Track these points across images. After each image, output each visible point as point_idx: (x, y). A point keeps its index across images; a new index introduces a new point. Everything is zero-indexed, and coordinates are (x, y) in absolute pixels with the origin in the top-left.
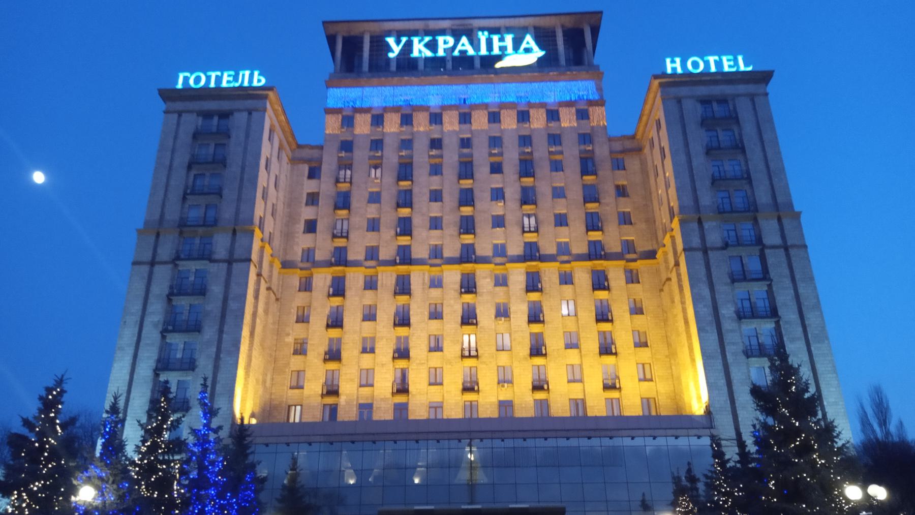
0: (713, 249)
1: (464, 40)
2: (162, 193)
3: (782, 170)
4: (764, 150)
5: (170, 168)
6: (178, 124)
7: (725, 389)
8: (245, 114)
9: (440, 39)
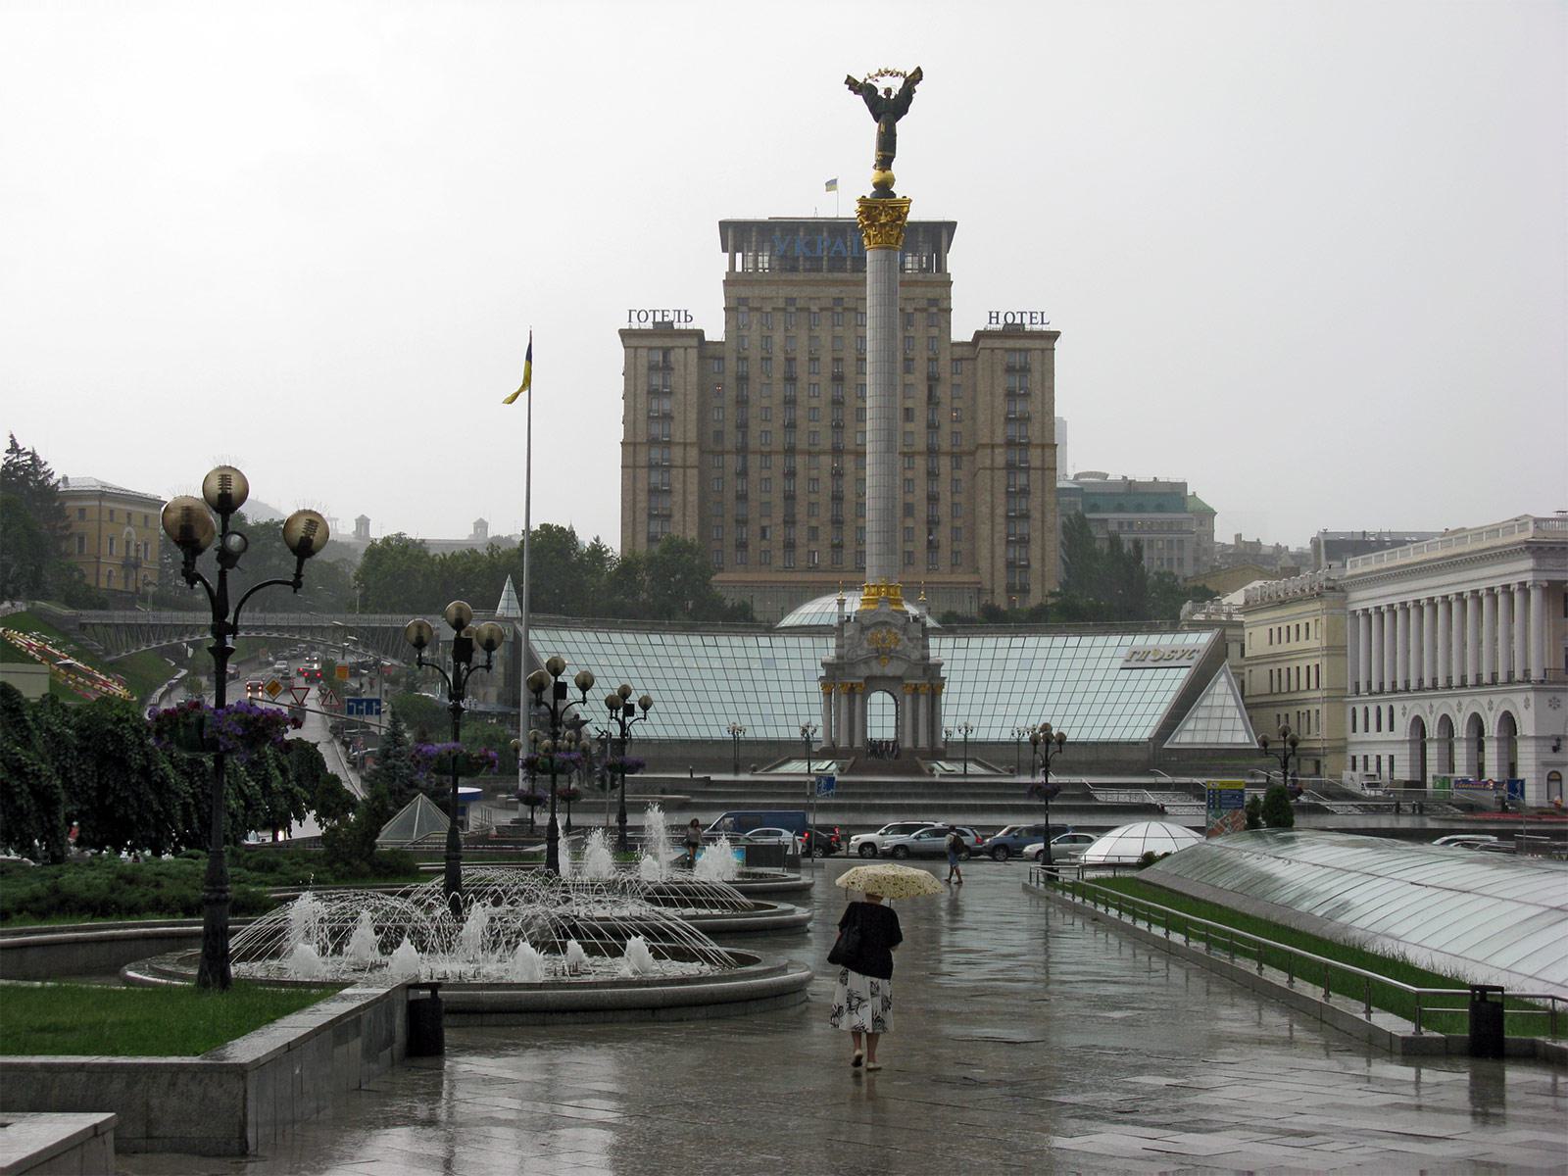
1: (839, 240)
4: (1043, 395)
5: (635, 395)
7: (989, 561)
8: (682, 350)
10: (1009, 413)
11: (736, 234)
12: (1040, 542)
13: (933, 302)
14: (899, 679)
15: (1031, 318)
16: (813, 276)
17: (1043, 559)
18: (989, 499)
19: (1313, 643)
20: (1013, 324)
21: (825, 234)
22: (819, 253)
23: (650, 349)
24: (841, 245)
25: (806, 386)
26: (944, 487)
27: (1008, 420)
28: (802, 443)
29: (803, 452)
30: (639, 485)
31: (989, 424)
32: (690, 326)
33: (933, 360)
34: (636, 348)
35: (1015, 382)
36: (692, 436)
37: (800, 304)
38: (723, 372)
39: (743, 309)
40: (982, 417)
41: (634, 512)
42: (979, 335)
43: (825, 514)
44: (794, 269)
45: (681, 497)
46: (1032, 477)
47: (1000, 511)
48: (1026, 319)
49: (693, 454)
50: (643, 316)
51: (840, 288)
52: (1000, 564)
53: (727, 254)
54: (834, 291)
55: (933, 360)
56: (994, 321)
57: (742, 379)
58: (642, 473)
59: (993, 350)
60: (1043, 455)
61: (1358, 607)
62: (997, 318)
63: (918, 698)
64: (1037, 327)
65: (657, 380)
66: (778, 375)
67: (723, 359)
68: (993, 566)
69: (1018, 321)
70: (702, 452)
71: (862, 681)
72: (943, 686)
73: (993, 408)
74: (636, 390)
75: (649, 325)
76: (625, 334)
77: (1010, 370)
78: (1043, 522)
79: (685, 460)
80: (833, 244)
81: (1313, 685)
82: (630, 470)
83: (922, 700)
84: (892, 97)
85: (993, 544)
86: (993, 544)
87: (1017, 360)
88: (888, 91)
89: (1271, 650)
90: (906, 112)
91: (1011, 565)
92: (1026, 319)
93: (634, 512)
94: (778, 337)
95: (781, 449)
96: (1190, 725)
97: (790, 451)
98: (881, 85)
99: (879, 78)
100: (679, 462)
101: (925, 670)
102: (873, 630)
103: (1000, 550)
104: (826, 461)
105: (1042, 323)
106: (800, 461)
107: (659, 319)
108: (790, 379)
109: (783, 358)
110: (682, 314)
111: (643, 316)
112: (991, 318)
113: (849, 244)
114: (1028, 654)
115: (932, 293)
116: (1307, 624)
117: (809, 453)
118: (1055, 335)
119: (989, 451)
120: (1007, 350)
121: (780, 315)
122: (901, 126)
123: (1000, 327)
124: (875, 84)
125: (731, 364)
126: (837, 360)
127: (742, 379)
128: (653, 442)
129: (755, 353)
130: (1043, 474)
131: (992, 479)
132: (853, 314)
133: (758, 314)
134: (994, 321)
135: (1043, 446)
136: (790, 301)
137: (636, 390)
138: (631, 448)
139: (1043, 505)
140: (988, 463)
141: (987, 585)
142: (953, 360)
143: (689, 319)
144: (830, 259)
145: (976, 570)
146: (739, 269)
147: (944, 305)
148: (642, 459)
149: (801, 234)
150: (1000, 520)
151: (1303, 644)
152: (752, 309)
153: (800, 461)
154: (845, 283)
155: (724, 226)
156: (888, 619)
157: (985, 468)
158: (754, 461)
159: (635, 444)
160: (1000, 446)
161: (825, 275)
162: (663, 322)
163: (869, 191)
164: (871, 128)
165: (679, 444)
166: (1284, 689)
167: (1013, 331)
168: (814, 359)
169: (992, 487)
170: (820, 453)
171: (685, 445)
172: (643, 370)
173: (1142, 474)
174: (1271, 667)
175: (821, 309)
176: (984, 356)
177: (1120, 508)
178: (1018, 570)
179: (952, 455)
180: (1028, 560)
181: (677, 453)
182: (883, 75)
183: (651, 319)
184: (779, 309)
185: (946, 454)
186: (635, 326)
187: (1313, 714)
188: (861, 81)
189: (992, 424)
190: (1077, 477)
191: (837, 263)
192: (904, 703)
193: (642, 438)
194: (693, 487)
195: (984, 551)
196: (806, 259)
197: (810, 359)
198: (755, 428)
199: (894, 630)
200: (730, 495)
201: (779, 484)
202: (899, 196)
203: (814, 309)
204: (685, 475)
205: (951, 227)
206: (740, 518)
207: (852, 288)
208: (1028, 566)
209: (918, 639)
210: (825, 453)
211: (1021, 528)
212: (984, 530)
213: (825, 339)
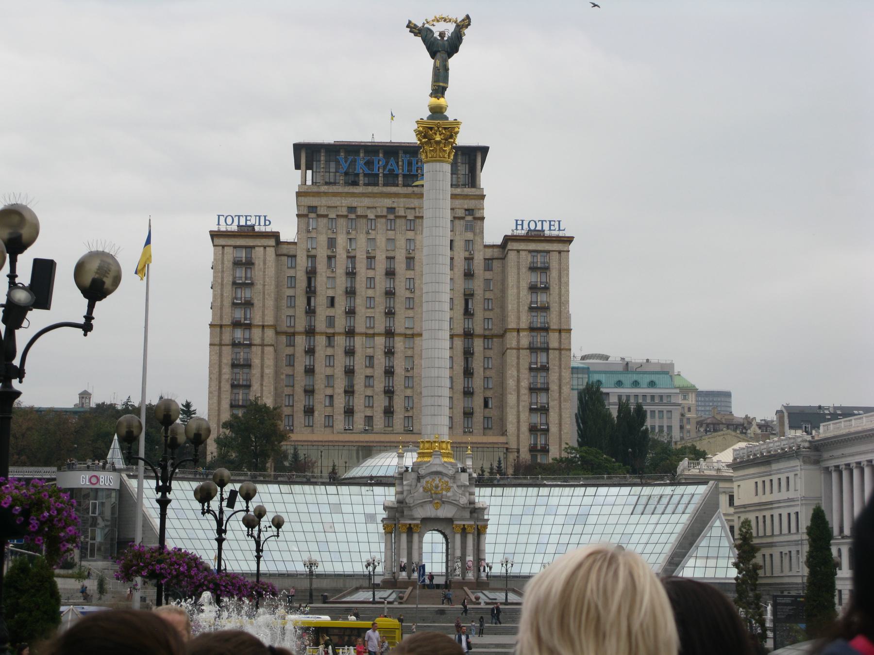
0: (523, 349)
1: (392, 161)
2: (219, 300)
3: (568, 302)
4: (560, 288)
6: (223, 253)
8: (262, 249)
9: (375, 159)
10: (531, 302)
11: (307, 154)
12: (557, 410)
13: (470, 211)
14: (450, 521)
15: (550, 225)
16: (370, 189)
17: (560, 425)
18: (515, 373)
19: (791, 494)
20: (535, 230)
21: (381, 155)
22: (375, 171)
23: (235, 247)
24: (394, 166)
25: (364, 279)
26: (477, 364)
27: (531, 309)
28: (360, 327)
29: (361, 334)
30: (225, 361)
31: (517, 313)
32: (268, 229)
33: (469, 259)
34: (223, 247)
35: (535, 278)
36: (270, 320)
37: (360, 212)
38: (295, 267)
39: (312, 215)
40: (511, 306)
41: (220, 382)
42: (507, 239)
43: (379, 385)
44: (355, 183)
45: (259, 370)
46: (551, 356)
47: (525, 384)
48: (546, 226)
49: (270, 334)
50: (229, 220)
51: (393, 200)
52: (524, 428)
53: (299, 171)
54: (388, 202)
55: (469, 259)
56: (519, 227)
57: (311, 274)
58: (227, 351)
59: (518, 251)
60: (560, 338)
61: (832, 463)
62: (522, 225)
63: (466, 537)
64: (555, 233)
65: (240, 273)
66: (340, 271)
67: (295, 256)
68: (519, 430)
69: (539, 228)
70: (277, 333)
71: (419, 522)
72: (486, 527)
73: (518, 298)
74: (222, 281)
75: (234, 228)
76: (214, 235)
77: (533, 269)
78: (560, 392)
79: (263, 340)
80: (387, 163)
81: (793, 530)
82: (217, 348)
83: (470, 539)
84: (446, 39)
85: (518, 411)
86: (518, 411)
87: (539, 260)
88: (442, 35)
89: (756, 500)
90: (457, 51)
91: (533, 429)
92: (546, 226)
93: (220, 382)
94: (341, 240)
95: (342, 330)
96: (691, 562)
97: (350, 333)
98: (436, 29)
99: (435, 23)
100: (257, 340)
101: (471, 513)
102: (428, 479)
103: (525, 415)
104: (380, 341)
105: (559, 230)
106: (359, 341)
107: (243, 223)
108: (351, 274)
109: (345, 256)
110: (262, 219)
111: (229, 220)
112: (517, 224)
113: (400, 163)
114: (553, 501)
115: (470, 204)
116: (788, 478)
117: (366, 335)
118: (569, 240)
119: (515, 334)
120: (530, 251)
121: (342, 222)
122: (453, 62)
123: (524, 232)
124: (432, 28)
125: (302, 262)
126: (391, 258)
127: (311, 274)
128: (236, 324)
129: (322, 253)
130: (560, 354)
131: (518, 358)
132: (403, 220)
133: (325, 220)
134: (519, 227)
135: (560, 331)
136: (352, 209)
137: (222, 281)
138: (218, 329)
139: (560, 380)
140: (514, 344)
141: (513, 445)
142: (485, 259)
143: (267, 223)
144: (385, 175)
145: (504, 433)
146: (309, 182)
147: (477, 215)
148: (227, 338)
149: (362, 155)
150: (524, 391)
151: (784, 495)
152: (319, 216)
153: (359, 341)
154: (397, 195)
155: (298, 148)
156: (440, 469)
157: (511, 349)
158: (320, 341)
159: (221, 326)
160: (524, 330)
161: (381, 189)
162: (246, 226)
163: (426, 114)
164: (428, 63)
165: (258, 326)
166: (769, 533)
167: (535, 236)
168: (371, 258)
169: (518, 364)
170: (374, 335)
171: (263, 326)
172: (228, 264)
173: (636, 357)
174: (757, 514)
175: (377, 217)
176: (512, 256)
177: (619, 384)
178: (539, 433)
179: (485, 337)
180: (547, 424)
181: (256, 334)
182: (438, 21)
183: (236, 223)
184: (342, 216)
185: (479, 336)
186: (223, 228)
187: (794, 554)
188: (420, 25)
189: (518, 311)
190: (583, 358)
191: (391, 179)
192: (454, 542)
193: (227, 321)
194: (269, 361)
195: (511, 417)
196: (365, 175)
197: (368, 258)
198: (322, 312)
199: (446, 479)
200: (300, 368)
201: (341, 361)
202: (451, 119)
203: (371, 216)
204: (263, 352)
205: (484, 150)
206: (307, 388)
207: (402, 200)
208: (547, 430)
209: (465, 486)
210: (379, 334)
211: (542, 398)
212: (511, 399)
213: (381, 240)
